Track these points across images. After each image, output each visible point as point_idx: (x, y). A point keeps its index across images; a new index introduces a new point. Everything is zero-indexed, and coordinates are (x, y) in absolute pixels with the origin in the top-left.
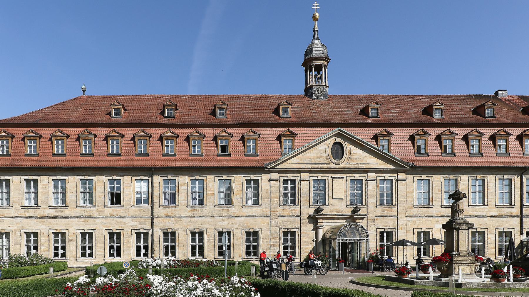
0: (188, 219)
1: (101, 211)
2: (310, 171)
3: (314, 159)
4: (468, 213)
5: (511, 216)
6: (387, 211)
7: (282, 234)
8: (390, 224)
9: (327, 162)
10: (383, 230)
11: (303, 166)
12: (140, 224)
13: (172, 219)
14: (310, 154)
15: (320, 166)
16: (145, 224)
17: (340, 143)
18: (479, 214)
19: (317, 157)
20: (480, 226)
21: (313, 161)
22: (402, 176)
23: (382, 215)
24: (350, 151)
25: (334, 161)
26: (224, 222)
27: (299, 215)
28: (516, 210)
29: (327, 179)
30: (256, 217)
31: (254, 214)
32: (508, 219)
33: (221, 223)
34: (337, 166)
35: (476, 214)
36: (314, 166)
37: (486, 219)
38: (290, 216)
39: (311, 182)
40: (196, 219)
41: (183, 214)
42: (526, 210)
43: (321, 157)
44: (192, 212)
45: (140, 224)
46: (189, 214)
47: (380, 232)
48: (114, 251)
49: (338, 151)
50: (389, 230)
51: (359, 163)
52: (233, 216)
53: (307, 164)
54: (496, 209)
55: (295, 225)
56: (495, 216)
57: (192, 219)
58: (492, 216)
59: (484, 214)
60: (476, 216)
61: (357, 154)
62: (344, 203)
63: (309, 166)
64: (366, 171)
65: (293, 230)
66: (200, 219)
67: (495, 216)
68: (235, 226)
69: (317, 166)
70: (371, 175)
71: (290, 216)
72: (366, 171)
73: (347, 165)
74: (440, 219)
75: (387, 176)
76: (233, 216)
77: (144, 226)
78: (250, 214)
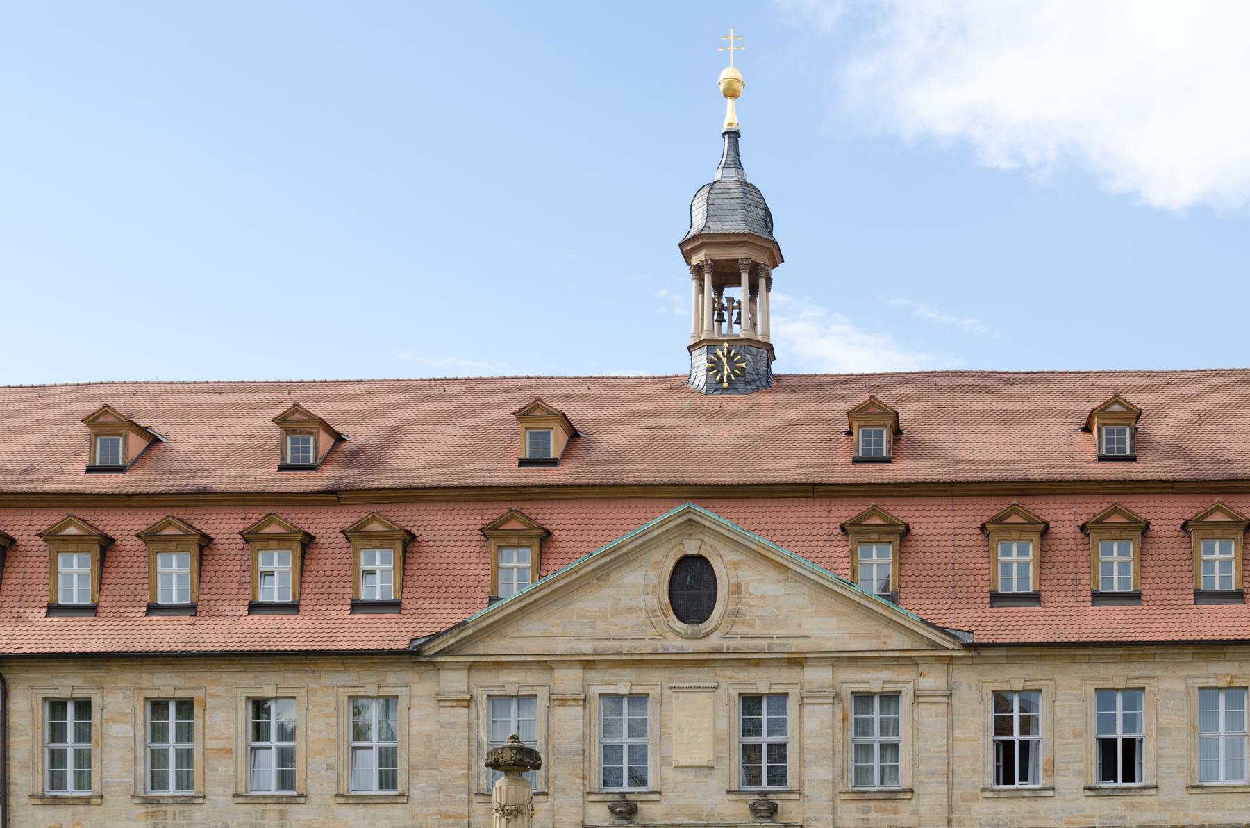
2: (587, 665)
9: (651, 631)
11: (561, 646)
14: (591, 602)
15: (626, 646)
17: (700, 559)
21: (601, 627)
22: (932, 680)
24: (737, 589)
29: (654, 692)
34: (691, 646)
39: (595, 704)
43: (630, 610)
49: (692, 589)
61: (763, 597)
63: (586, 647)
64: (797, 661)
69: (614, 645)
70: (817, 676)
72: (797, 661)
73: (730, 644)
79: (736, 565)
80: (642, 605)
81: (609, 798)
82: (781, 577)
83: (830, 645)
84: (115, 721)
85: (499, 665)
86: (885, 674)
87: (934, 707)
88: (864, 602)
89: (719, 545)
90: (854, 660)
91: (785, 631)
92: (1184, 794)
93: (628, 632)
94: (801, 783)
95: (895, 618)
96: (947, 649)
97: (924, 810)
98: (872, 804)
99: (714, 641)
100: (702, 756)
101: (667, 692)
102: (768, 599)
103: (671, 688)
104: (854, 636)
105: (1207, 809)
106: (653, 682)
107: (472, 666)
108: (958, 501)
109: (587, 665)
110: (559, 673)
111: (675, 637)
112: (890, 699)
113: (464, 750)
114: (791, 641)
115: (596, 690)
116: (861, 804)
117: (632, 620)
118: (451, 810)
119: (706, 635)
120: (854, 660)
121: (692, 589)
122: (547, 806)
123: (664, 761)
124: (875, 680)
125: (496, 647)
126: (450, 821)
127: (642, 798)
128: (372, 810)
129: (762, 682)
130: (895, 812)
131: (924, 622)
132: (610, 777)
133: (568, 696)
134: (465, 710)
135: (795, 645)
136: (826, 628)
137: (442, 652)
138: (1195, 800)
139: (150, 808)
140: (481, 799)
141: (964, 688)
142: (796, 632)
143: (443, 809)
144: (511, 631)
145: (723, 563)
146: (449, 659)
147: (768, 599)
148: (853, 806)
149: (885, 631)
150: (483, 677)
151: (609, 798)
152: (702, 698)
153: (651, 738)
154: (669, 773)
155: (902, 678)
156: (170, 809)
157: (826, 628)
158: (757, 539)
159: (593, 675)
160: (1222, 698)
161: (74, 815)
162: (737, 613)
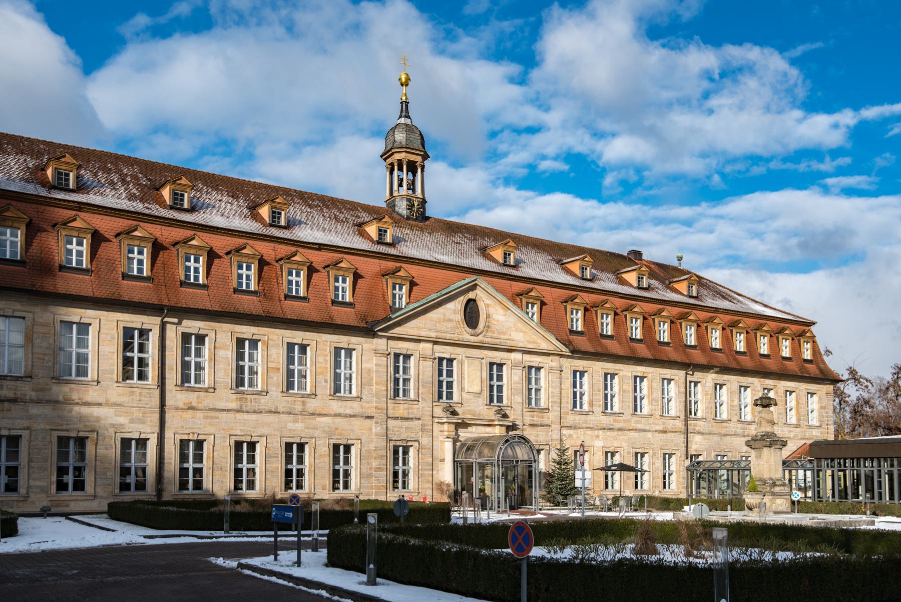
0: (232, 415)
1: (42, 390)
2: (435, 343)
5: (675, 432)
6: (537, 416)
11: (423, 333)
12: (132, 421)
13: (199, 415)
15: (448, 336)
16: (143, 423)
19: (444, 320)
21: (439, 326)
22: (553, 362)
24: (488, 316)
26: (296, 425)
30: (351, 416)
31: (348, 412)
33: (290, 426)
34: (473, 339)
35: (639, 426)
37: (649, 435)
38: (407, 419)
40: (246, 416)
41: (221, 405)
43: (450, 320)
44: (239, 403)
45: (132, 421)
46: (234, 405)
48: (70, 479)
49: (471, 315)
51: (502, 337)
52: (313, 414)
53: (430, 330)
54: (660, 422)
55: (413, 435)
57: (239, 416)
59: (647, 428)
60: (640, 430)
63: (433, 335)
66: (254, 417)
68: (317, 433)
69: (443, 335)
71: (407, 419)
73: (486, 339)
74: (601, 432)
75: (535, 360)
76: (313, 414)
77: (141, 426)
78: (342, 411)
83: (521, 345)
84: (221, 348)
91: (505, 337)
99: (480, 338)
100: (476, 389)
106: (458, 353)
107: (389, 338)
111: (466, 335)
112: (500, 366)
117: (450, 325)
121: (471, 315)
124: (535, 360)
128: (344, 403)
129: (497, 357)
135: (509, 343)
137: (379, 331)
139: (239, 396)
150: (392, 343)
156: (249, 397)
160: (75, 326)
161: (198, 397)
162: (489, 327)
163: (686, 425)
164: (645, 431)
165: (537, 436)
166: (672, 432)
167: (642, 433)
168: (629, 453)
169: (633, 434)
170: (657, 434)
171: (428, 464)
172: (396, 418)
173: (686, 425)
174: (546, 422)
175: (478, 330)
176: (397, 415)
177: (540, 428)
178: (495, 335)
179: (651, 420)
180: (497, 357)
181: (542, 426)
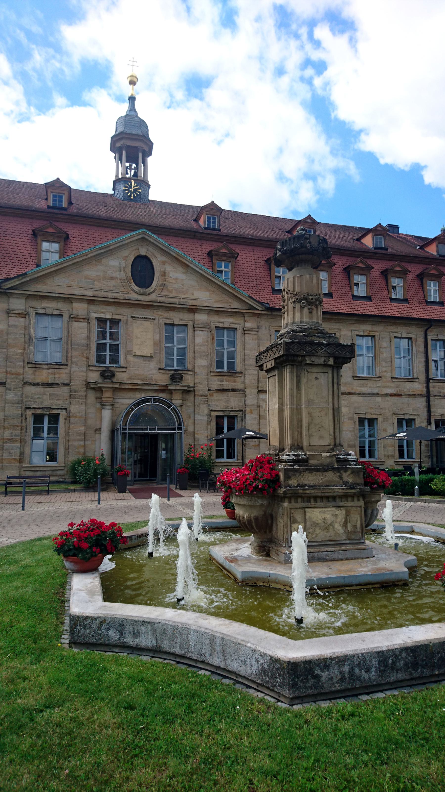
2: (91, 302)
3: (99, 280)
4: (352, 389)
5: (414, 395)
7: (31, 420)
8: (233, 402)
9: (122, 289)
10: (221, 414)
11: (76, 292)
14: (92, 272)
15: (110, 295)
17: (146, 258)
18: (369, 391)
19: (105, 278)
20: (369, 411)
21: (97, 285)
23: (220, 387)
24: (164, 274)
25: (136, 288)
27: (67, 382)
28: (419, 387)
29: (123, 318)
32: (410, 399)
35: (364, 390)
36: (98, 293)
37: (379, 399)
38: (51, 385)
39: (94, 323)
42: (434, 387)
43: (112, 278)
47: (217, 417)
49: (142, 271)
50: (232, 414)
53: (85, 288)
54: (393, 384)
56: (392, 395)
58: (387, 395)
59: (376, 391)
60: (364, 394)
61: (176, 279)
62: (153, 365)
63: (90, 293)
64: (192, 310)
65: (55, 412)
67: (392, 395)
70: (201, 318)
71: (51, 385)
72: (192, 310)
73: (159, 299)
75: (227, 321)
79: (164, 263)
80: (118, 276)
81: (100, 369)
82: (184, 271)
85: (43, 297)
86: (230, 320)
87: (251, 336)
88: (223, 286)
89: (155, 252)
90: (217, 312)
92: (351, 379)
93: (111, 288)
94: (194, 367)
95: (236, 294)
96: (257, 310)
97: (247, 381)
98: (225, 378)
99: (153, 297)
100: (147, 351)
101: (130, 319)
102: (177, 281)
103: (132, 317)
104: (216, 301)
105: (361, 387)
106: (123, 314)
107: (29, 297)
108: (255, 248)
109: (91, 302)
110: (75, 305)
111: (134, 293)
113: (22, 340)
114: (189, 301)
115: (94, 315)
116: (220, 378)
117: (113, 283)
118: (13, 370)
119: (150, 294)
120: (217, 312)
121: (142, 271)
122: (67, 371)
123: (129, 352)
124: (227, 321)
125: (41, 288)
126: (13, 376)
127: (118, 369)
130: (235, 382)
131: (249, 296)
132: (101, 359)
133: (80, 317)
134: (23, 320)
136: (204, 296)
138: (356, 383)
140: (30, 366)
141: (264, 328)
142: (191, 297)
143: (9, 369)
144: (49, 281)
145: (157, 261)
146: (12, 291)
147: (177, 281)
148: (216, 378)
149: (230, 300)
151: (100, 369)
152: (147, 324)
153: (122, 342)
154: (131, 359)
155: (237, 322)
157: (204, 296)
158: (176, 250)
159: (92, 307)
163: (428, 387)
164: (372, 394)
165: (228, 401)
166: (409, 395)
167: (368, 398)
168: (350, 419)
169: (354, 398)
170: (388, 398)
171: (78, 434)
172: (36, 384)
173: (428, 387)
174: (240, 386)
175: (151, 289)
176: (37, 381)
177: (231, 394)
178: (173, 294)
179: (379, 384)
180: (177, 318)
181: (233, 390)
